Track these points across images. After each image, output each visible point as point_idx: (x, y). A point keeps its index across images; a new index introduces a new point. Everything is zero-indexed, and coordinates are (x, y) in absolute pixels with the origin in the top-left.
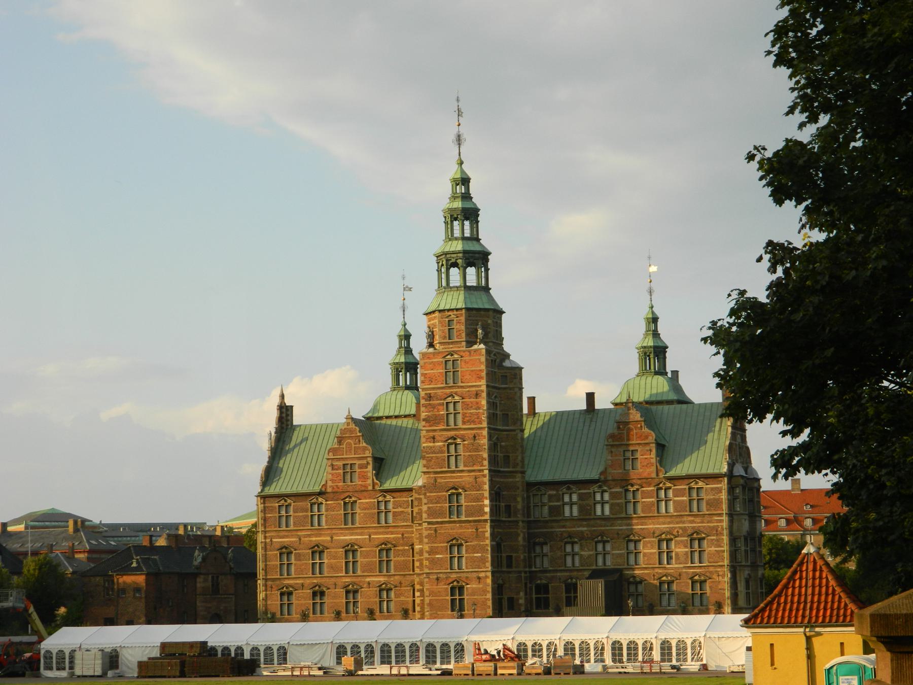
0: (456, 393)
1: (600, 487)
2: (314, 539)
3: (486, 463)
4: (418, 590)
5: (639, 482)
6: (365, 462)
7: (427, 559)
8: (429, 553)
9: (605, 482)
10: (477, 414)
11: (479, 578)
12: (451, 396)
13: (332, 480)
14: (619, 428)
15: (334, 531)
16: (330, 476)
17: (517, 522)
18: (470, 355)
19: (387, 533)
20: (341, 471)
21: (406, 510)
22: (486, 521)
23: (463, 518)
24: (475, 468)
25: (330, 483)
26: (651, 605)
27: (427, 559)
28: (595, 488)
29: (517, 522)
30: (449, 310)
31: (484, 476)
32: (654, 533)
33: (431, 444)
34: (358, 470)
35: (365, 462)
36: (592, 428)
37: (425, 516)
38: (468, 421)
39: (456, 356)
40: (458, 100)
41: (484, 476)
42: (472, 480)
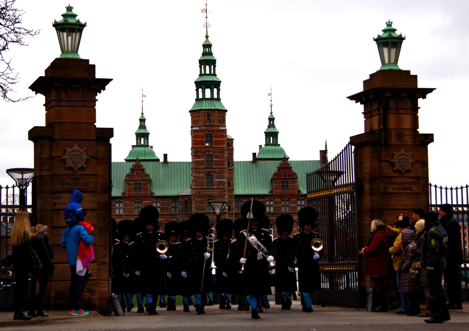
3: (226, 185)
5: (289, 196)
9: (272, 195)
10: (222, 161)
12: (209, 152)
13: (128, 191)
16: (127, 189)
20: (133, 187)
21: (168, 207)
22: (226, 213)
25: (127, 192)
28: (267, 199)
29: (232, 214)
31: (226, 191)
33: (198, 175)
34: (142, 186)
35: (146, 182)
36: (258, 170)
37: (193, 209)
39: (211, 132)
40: (206, 5)
41: (226, 191)
42: (218, 193)
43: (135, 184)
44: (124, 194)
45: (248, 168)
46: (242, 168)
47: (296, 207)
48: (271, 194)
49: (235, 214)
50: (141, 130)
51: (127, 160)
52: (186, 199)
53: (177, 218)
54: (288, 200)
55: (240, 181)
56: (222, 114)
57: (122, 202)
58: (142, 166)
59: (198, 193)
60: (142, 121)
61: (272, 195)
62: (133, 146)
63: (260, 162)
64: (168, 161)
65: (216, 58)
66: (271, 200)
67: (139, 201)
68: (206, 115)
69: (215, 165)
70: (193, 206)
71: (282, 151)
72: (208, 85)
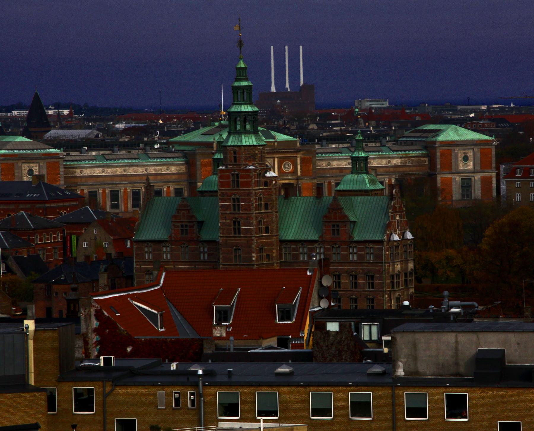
0: (237, 193)
6: (192, 224)
12: (234, 194)
14: (329, 212)
16: (173, 231)
17: (273, 264)
25: (173, 235)
28: (316, 245)
30: (233, 146)
31: (253, 240)
32: (347, 271)
35: (192, 224)
37: (221, 260)
43: (182, 226)
44: (170, 237)
45: (310, 206)
46: (303, 206)
47: (347, 256)
48: (320, 240)
55: (296, 222)
56: (252, 149)
61: (321, 242)
68: (232, 152)
69: (242, 211)
70: (221, 256)
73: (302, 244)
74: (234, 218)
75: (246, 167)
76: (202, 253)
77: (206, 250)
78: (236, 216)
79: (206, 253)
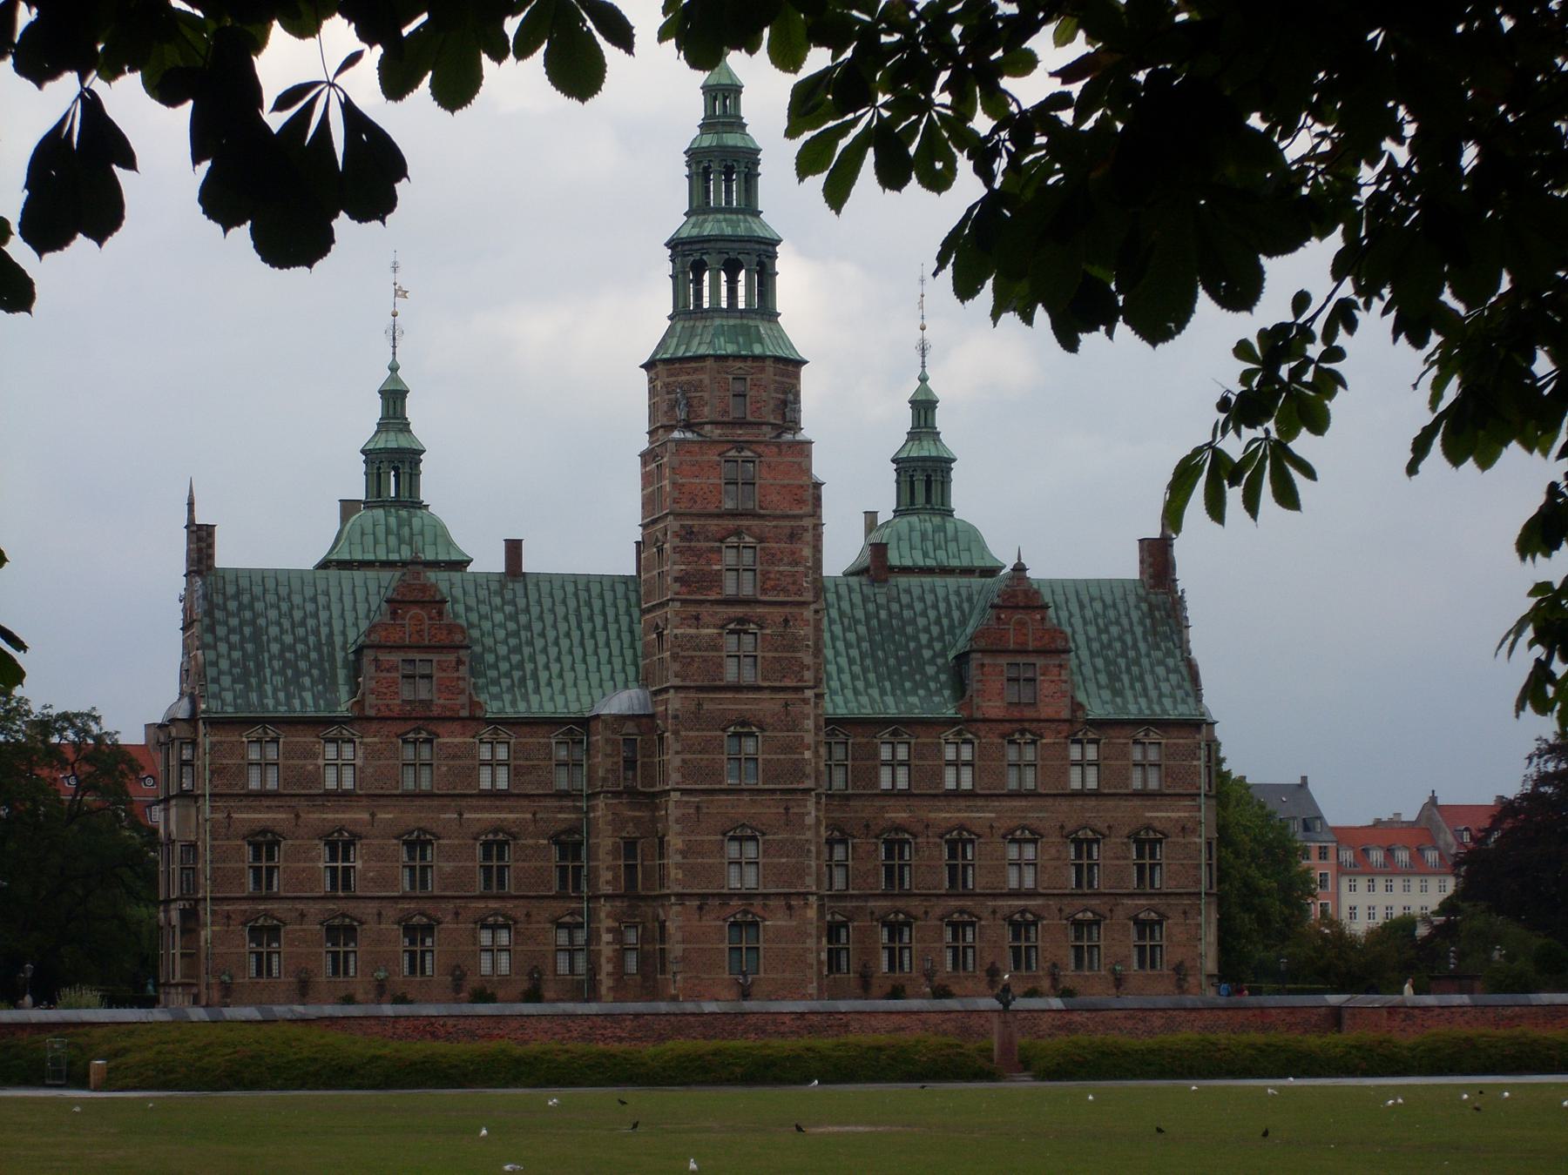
1: (959, 733)
2: (330, 816)
4: (609, 930)
7: (679, 866)
8: (684, 854)
11: (790, 907)
12: (738, 533)
15: (383, 802)
18: (780, 453)
19: (499, 809)
22: (807, 791)
23: (761, 786)
24: (787, 683)
26: (1055, 965)
27: (679, 866)
28: (949, 734)
31: (805, 701)
32: (1062, 827)
33: (693, 631)
35: (452, 657)
37: (675, 778)
38: (774, 588)
49: (827, 796)
50: (392, 435)
51: (325, 565)
52: (630, 728)
53: (578, 809)
54: (1034, 742)
57: (351, 741)
58: (435, 587)
59: (693, 708)
60: (394, 398)
62: (348, 507)
63: (903, 581)
64: (527, 567)
65: (759, 144)
66: (966, 742)
67: (424, 735)
71: (972, 537)
72: (732, 255)
73: (894, 734)
74: (731, 621)
75: (779, 436)
76: (484, 763)
77: (502, 753)
78: (739, 611)
79: (501, 764)
